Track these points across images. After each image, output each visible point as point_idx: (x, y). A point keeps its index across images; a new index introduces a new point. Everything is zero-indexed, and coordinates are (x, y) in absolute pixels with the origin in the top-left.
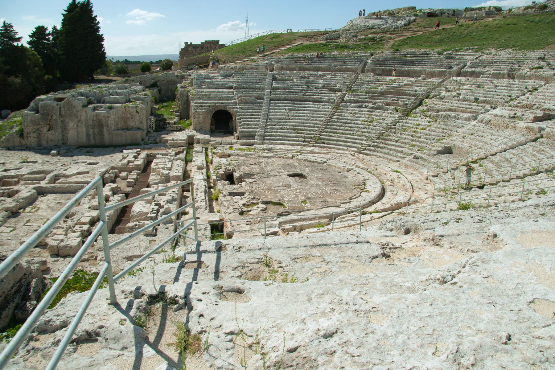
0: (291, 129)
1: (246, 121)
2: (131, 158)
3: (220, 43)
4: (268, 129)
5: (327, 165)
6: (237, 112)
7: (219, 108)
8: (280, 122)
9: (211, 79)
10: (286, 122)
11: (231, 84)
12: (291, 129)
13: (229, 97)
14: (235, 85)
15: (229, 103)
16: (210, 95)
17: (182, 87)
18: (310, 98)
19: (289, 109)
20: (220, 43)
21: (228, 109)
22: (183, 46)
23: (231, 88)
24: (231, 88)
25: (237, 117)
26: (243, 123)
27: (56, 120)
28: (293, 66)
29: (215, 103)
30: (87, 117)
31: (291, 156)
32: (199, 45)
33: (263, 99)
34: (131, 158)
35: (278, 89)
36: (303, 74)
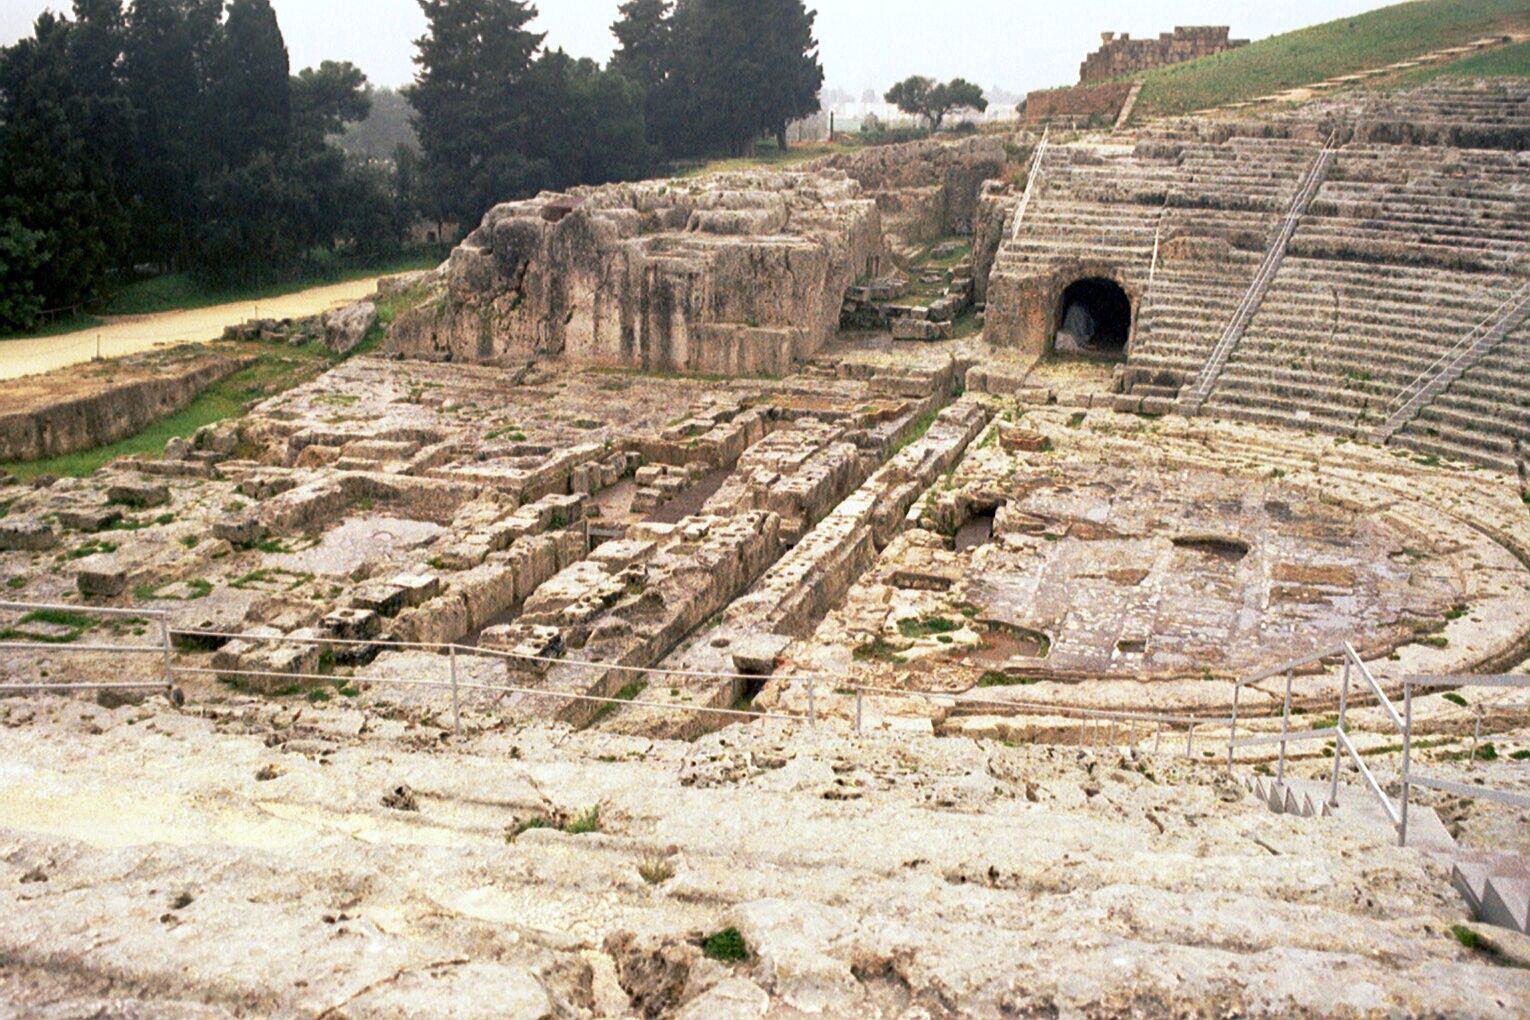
0: (1328, 369)
1: (1167, 325)
2: (705, 419)
3: (1232, 36)
4: (1239, 359)
5: (1386, 520)
6: (1145, 288)
7: (1091, 273)
8: (1292, 338)
9: (1099, 163)
10: (1317, 339)
11: (1159, 187)
12: (1328, 369)
13: (1137, 234)
14: (1172, 191)
15: (1130, 254)
16: (1072, 222)
17: (994, 190)
18: (1444, 251)
19: (1347, 292)
20: (1232, 36)
21: (1119, 278)
22: (1096, 45)
23: (1158, 200)
24: (1158, 200)
25: (1143, 310)
26: (1154, 331)
27: (538, 277)
28: (1429, 122)
29: (1077, 252)
30: (626, 274)
31: (1268, 468)
32: (1152, 42)
33: (1261, 248)
34: (705, 419)
35: (1332, 211)
36: (1453, 156)
